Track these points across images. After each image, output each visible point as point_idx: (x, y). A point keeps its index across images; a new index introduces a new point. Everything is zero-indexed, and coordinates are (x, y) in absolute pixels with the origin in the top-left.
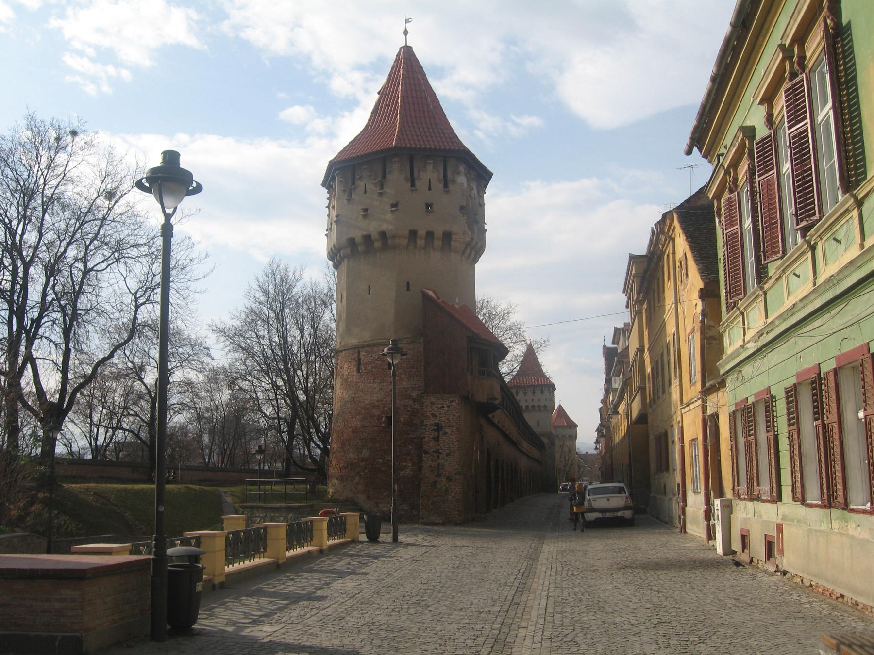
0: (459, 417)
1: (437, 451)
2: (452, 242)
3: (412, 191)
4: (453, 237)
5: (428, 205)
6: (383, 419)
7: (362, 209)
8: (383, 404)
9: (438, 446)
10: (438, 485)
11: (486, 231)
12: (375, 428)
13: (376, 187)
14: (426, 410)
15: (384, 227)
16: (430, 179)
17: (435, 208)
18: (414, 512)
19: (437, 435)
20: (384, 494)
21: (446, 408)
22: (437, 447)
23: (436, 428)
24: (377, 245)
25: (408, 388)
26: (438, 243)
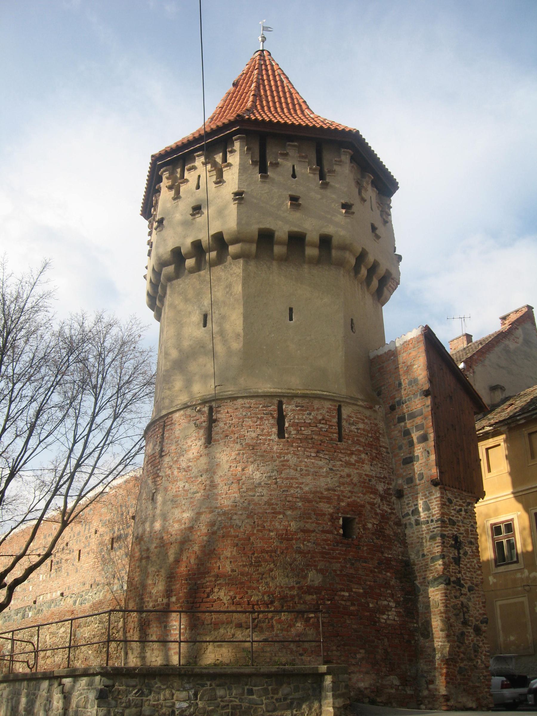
12: (330, 536)
13: (314, 174)
15: (330, 230)
18: (409, 691)
20: (358, 656)
21: (463, 513)
24: (311, 252)
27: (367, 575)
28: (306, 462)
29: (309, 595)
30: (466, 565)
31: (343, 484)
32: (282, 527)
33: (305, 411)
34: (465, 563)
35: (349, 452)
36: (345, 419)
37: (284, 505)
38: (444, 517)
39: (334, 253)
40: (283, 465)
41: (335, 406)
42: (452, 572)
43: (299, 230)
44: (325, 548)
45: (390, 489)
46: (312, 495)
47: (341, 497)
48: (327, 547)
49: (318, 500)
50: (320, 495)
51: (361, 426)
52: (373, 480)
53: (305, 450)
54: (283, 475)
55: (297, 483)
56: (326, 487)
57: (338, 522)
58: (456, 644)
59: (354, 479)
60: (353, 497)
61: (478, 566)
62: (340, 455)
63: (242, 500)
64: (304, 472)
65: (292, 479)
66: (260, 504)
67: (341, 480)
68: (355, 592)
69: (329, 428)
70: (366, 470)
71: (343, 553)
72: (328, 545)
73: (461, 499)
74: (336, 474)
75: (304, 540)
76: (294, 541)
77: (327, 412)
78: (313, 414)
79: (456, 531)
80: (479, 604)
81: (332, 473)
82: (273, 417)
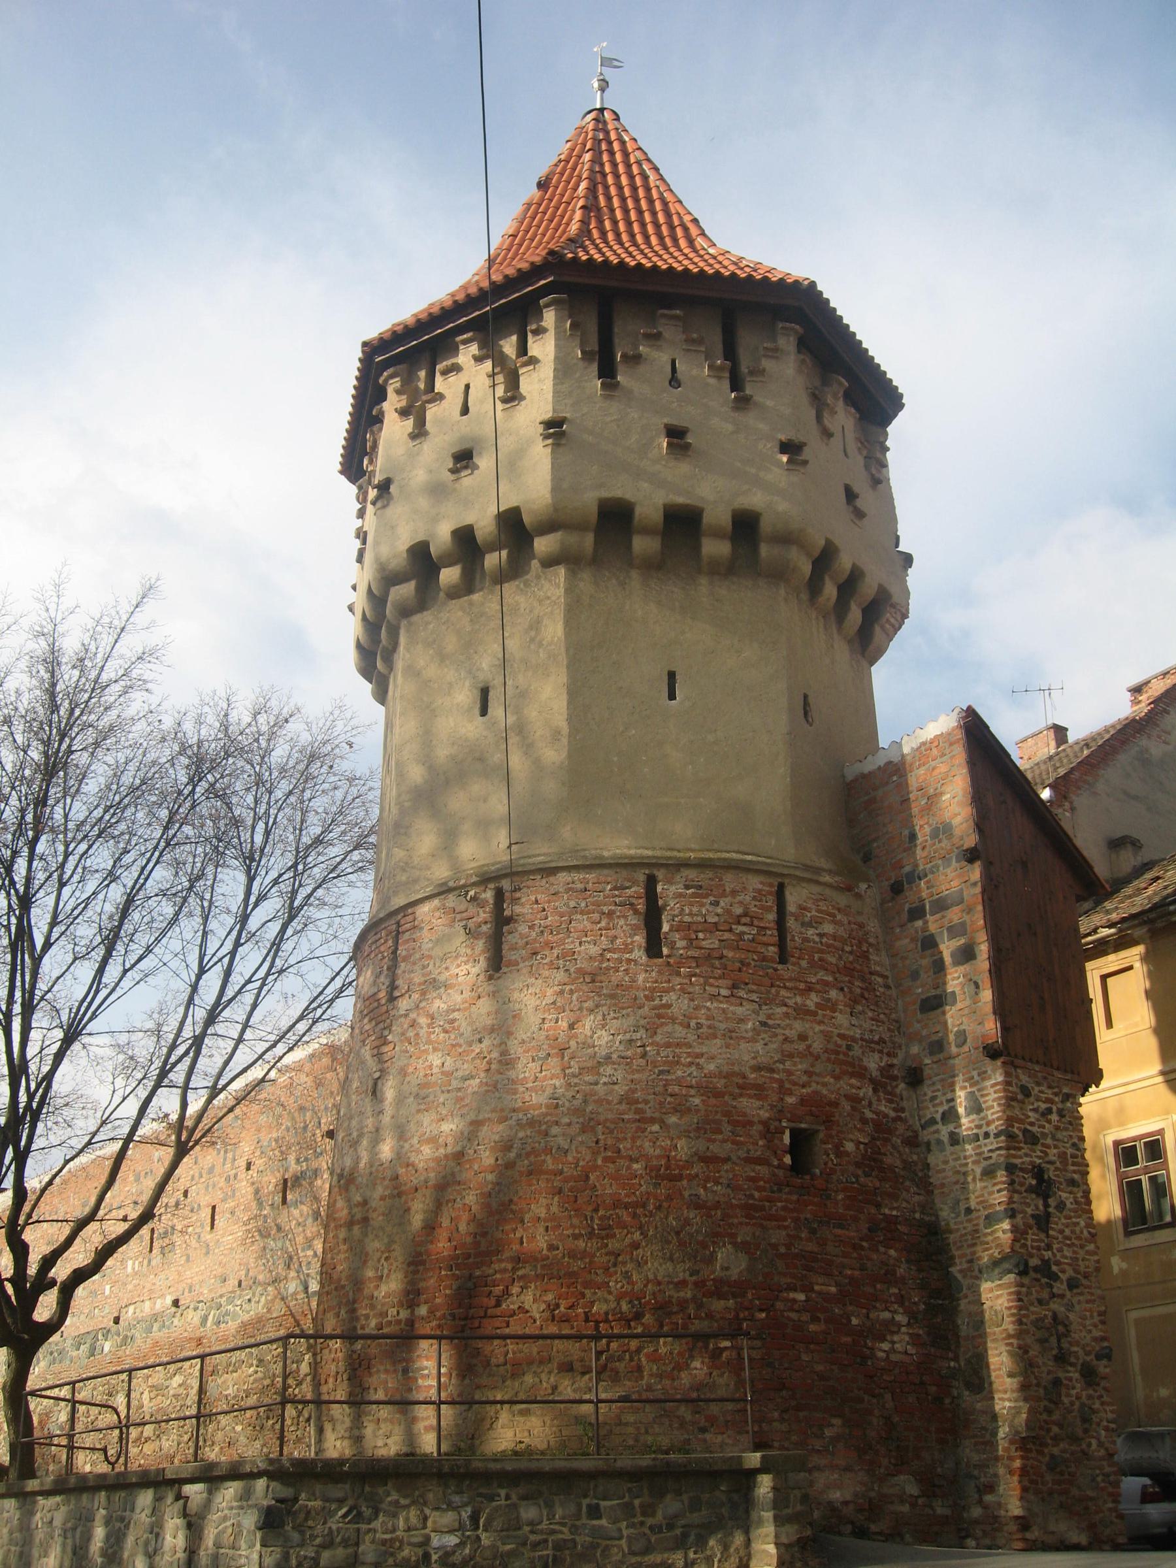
7: (666, 426)
8: (781, 1082)
12: (763, 1170)
13: (719, 378)
15: (755, 500)
18: (941, 1509)
21: (1054, 1117)
24: (715, 548)
28: (709, 1009)
29: (719, 1299)
30: (1061, 1232)
31: (791, 1056)
32: (658, 1152)
33: (706, 896)
34: (1060, 1226)
35: (802, 986)
36: (792, 914)
37: (661, 1103)
38: (1013, 1126)
40: (659, 1016)
41: (771, 885)
42: (1032, 1247)
43: (689, 502)
44: (751, 1196)
45: (892, 1066)
46: (723, 1081)
47: (787, 1085)
48: (757, 1194)
49: (737, 1091)
50: (741, 1081)
51: (828, 928)
52: (856, 1047)
53: (705, 983)
54: (658, 1038)
56: (753, 1062)
57: (782, 1140)
59: (815, 1045)
60: (814, 1085)
61: (1089, 1233)
62: (783, 992)
63: (569, 1094)
64: (704, 1030)
65: (678, 1045)
66: (609, 1102)
67: (786, 1047)
68: (820, 1293)
69: (758, 934)
70: (841, 1026)
71: (791, 1206)
72: (759, 1189)
73: (1050, 1087)
75: (707, 1180)
76: (685, 1182)
77: (754, 898)
78: (722, 904)
80: (1092, 1317)
81: (765, 1032)
82: (636, 912)
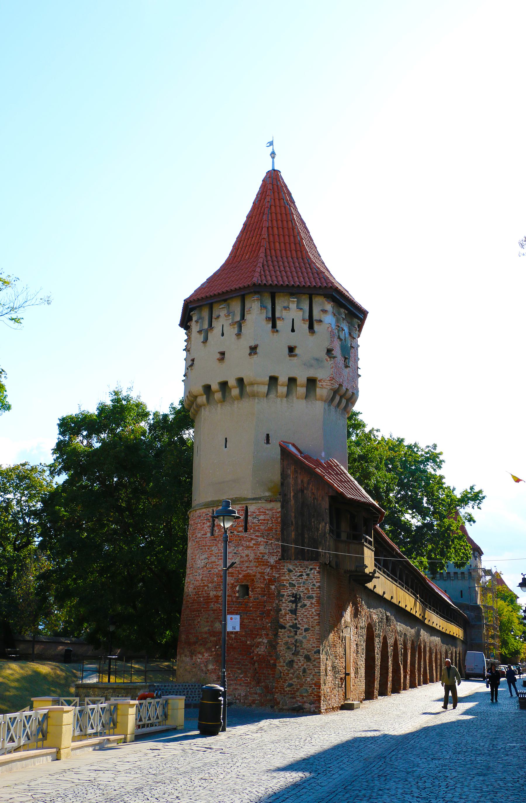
0: (319, 586)
1: (295, 626)
2: (318, 389)
3: (273, 332)
4: (319, 384)
5: (291, 350)
6: (237, 588)
8: (238, 571)
9: (296, 619)
10: (295, 665)
11: (360, 376)
13: (234, 328)
14: (283, 578)
16: (293, 319)
17: (297, 351)
19: (294, 607)
21: (305, 577)
22: (295, 622)
23: (294, 599)
24: (235, 392)
25: (265, 553)
26: (301, 390)
27: (250, 622)
34: (302, 612)
36: (249, 516)
39: (248, 389)
42: (289, 620)
47: (240, 572)
51: (262, 517)
52: (266, 556)
55: (215, 565)
57: (236, 589)
58: (285, 668)
66: (198, 581)
67: (242, 560)
73: (301, 567)
74: (238, 556)
79: (296, 591)
